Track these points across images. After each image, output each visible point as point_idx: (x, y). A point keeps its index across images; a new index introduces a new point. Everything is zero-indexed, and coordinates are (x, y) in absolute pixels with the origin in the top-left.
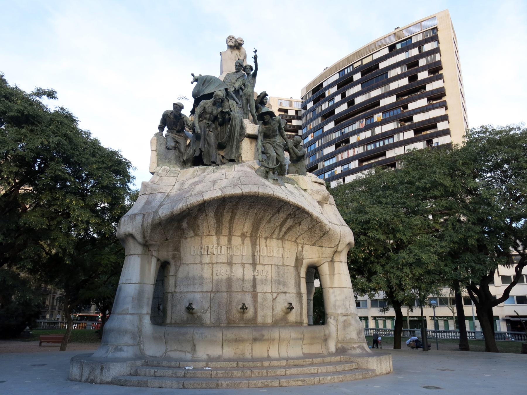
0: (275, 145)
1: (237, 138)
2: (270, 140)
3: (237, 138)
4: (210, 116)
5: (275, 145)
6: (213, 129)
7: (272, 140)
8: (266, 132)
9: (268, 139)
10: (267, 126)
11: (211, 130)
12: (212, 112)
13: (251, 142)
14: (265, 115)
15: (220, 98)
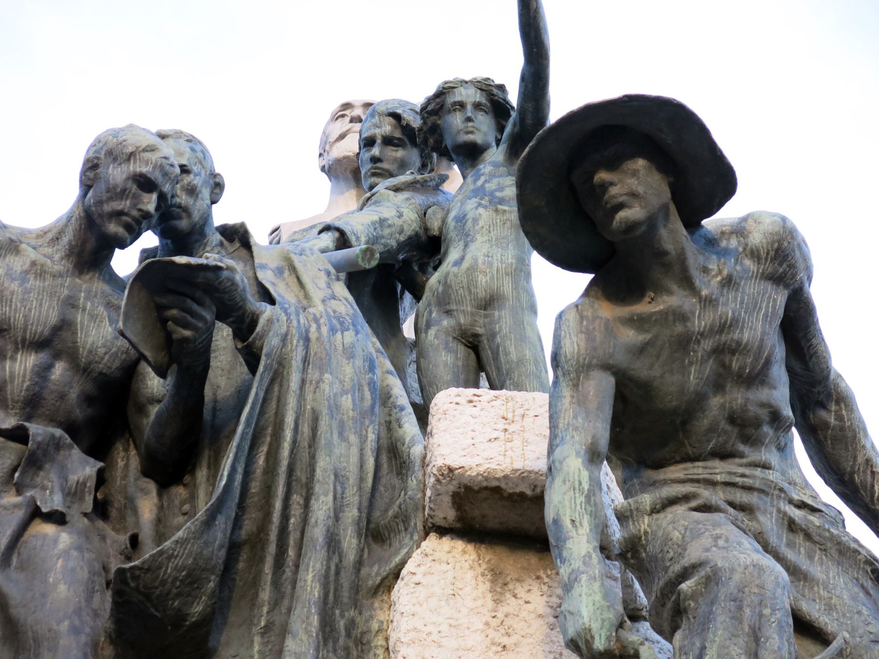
0: (768, 522)
1: (333, 543)
2: (698, 469)
3: (333, 543)
4: (43, 371)
5: (768, 522)
6: (73, 494)
7: (720, 470)
8: (642, 369)
9: (675, 472)
10: (643, 308)
11: (54, 501)
12: (64, 326)
13: (498, 579)
14: (613, 165)
15: (145, 183)
